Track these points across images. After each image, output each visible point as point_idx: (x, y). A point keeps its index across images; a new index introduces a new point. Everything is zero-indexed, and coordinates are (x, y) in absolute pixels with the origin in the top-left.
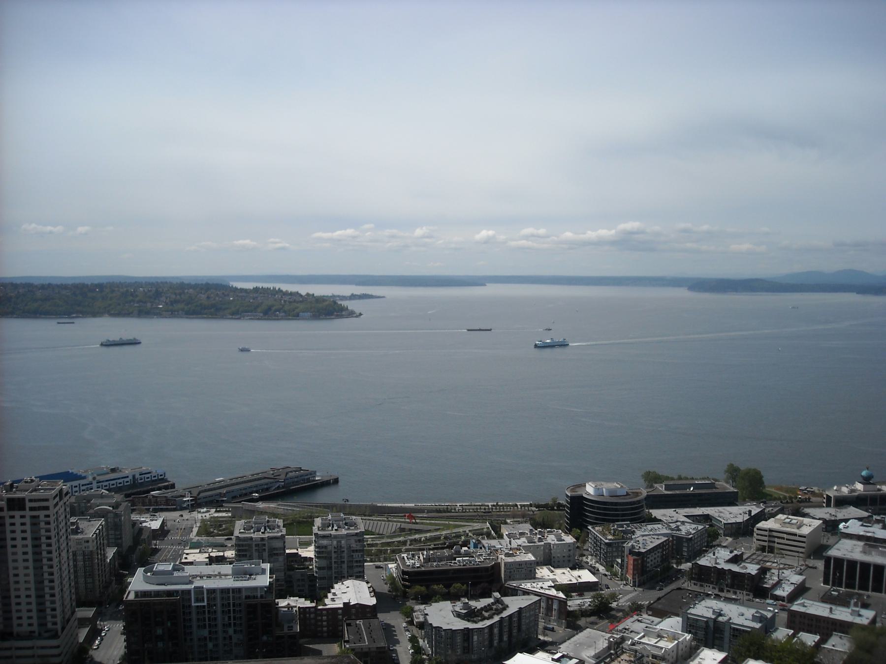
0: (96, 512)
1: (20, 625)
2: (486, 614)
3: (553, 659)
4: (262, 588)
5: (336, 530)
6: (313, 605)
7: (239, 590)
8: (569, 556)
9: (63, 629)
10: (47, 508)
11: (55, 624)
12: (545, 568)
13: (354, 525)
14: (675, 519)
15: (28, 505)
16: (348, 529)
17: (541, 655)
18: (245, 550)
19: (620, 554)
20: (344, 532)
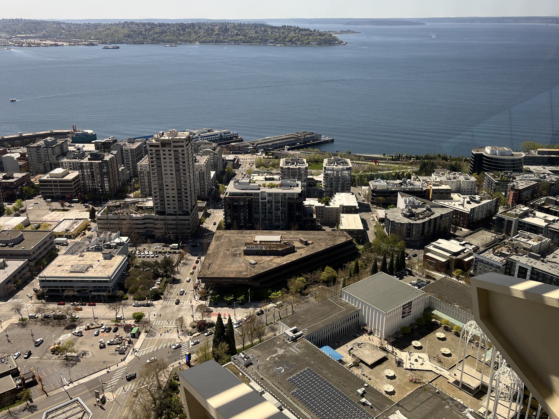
0: (204, 152)
1: (169, 208)
2: (421, 216)
3: (460, 244)
4: (296, 193)
5: (336, 166)
6: (323, 205)
7: (285, 194)
8: (472, 189)
9: (192, 211)
10: (183, 147)
11: (187, 208)
12: (456, 194)
13: (347, 163)
14: (542, 172)
15: (173, 144)
16: (343, 165)
17: (453, 241)
18: (287, 174)
19: (504, 190)
20: (341, 167)
